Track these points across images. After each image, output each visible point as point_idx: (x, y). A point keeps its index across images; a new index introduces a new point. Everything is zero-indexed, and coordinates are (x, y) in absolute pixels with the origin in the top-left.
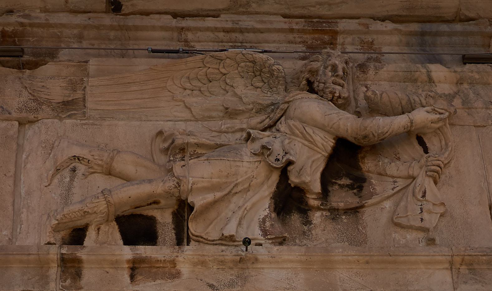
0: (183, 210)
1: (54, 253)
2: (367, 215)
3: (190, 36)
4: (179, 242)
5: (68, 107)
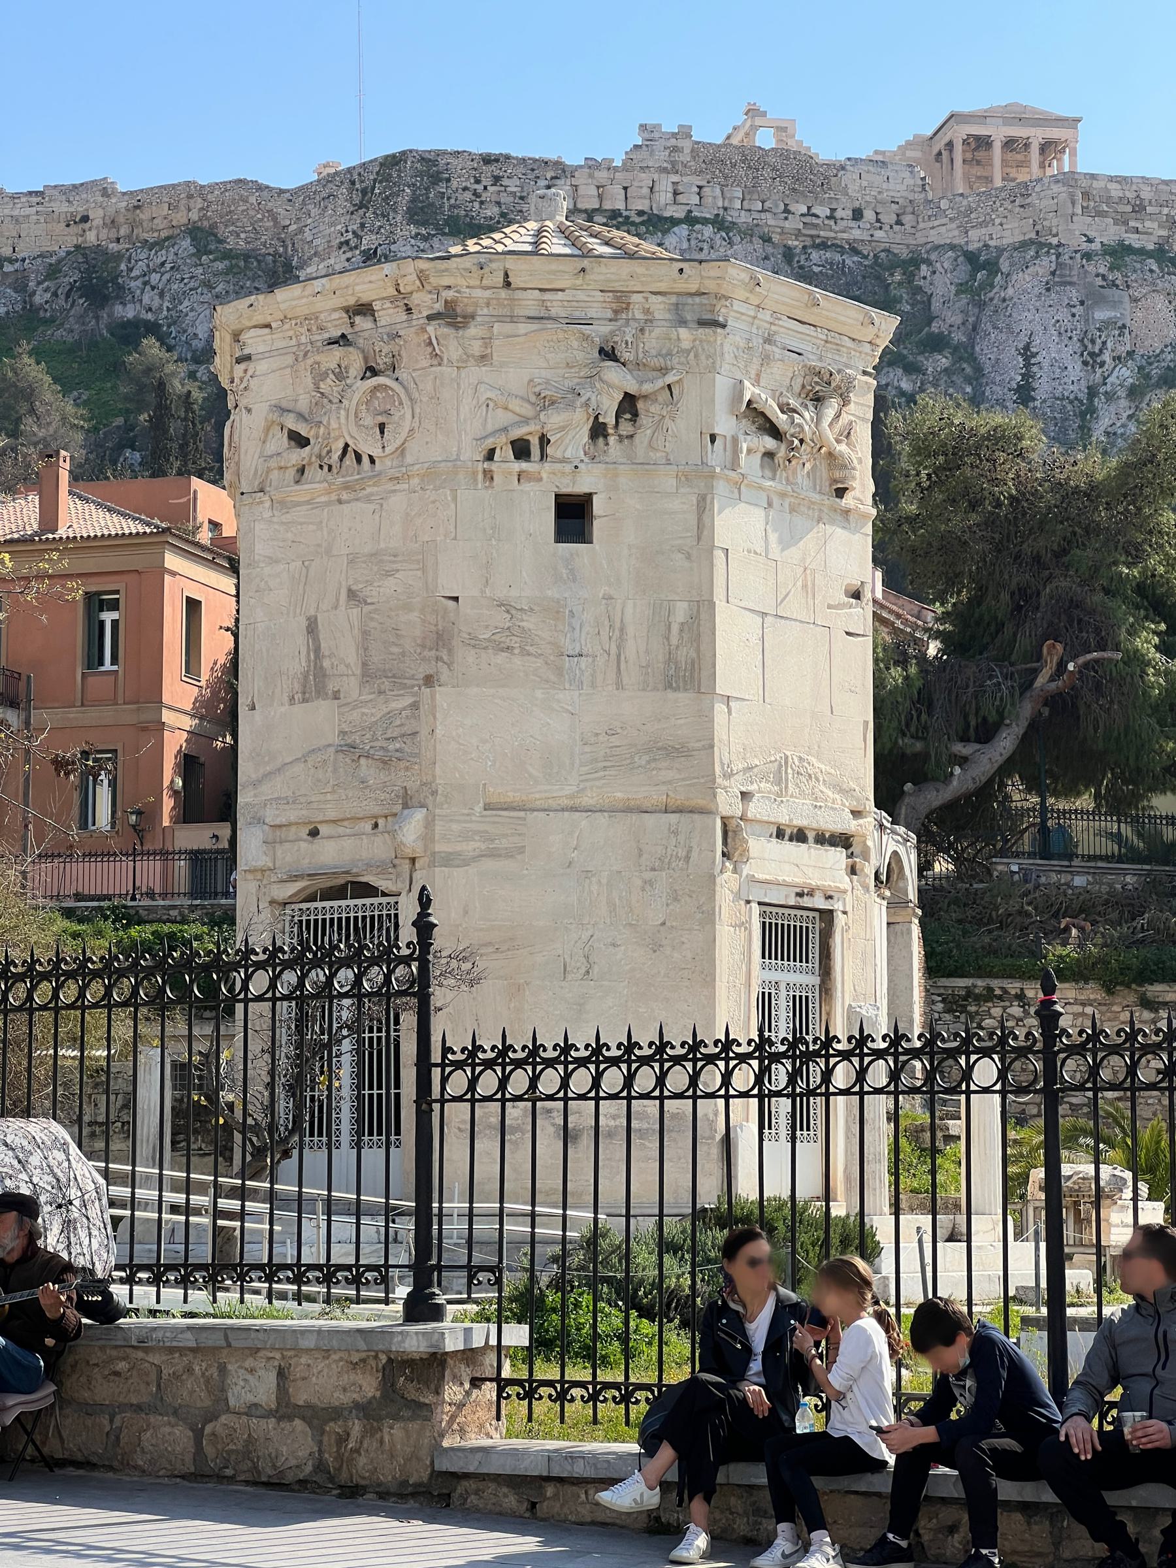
0: (544, 441)
1: (480, 467)
2: (637, 437)
3: (549, 304)
4: (542, 459)
5: (483, 358)
